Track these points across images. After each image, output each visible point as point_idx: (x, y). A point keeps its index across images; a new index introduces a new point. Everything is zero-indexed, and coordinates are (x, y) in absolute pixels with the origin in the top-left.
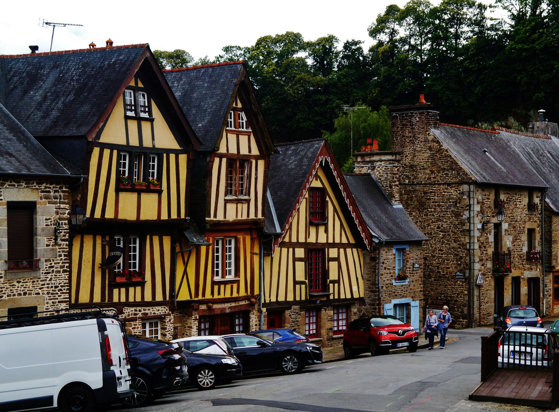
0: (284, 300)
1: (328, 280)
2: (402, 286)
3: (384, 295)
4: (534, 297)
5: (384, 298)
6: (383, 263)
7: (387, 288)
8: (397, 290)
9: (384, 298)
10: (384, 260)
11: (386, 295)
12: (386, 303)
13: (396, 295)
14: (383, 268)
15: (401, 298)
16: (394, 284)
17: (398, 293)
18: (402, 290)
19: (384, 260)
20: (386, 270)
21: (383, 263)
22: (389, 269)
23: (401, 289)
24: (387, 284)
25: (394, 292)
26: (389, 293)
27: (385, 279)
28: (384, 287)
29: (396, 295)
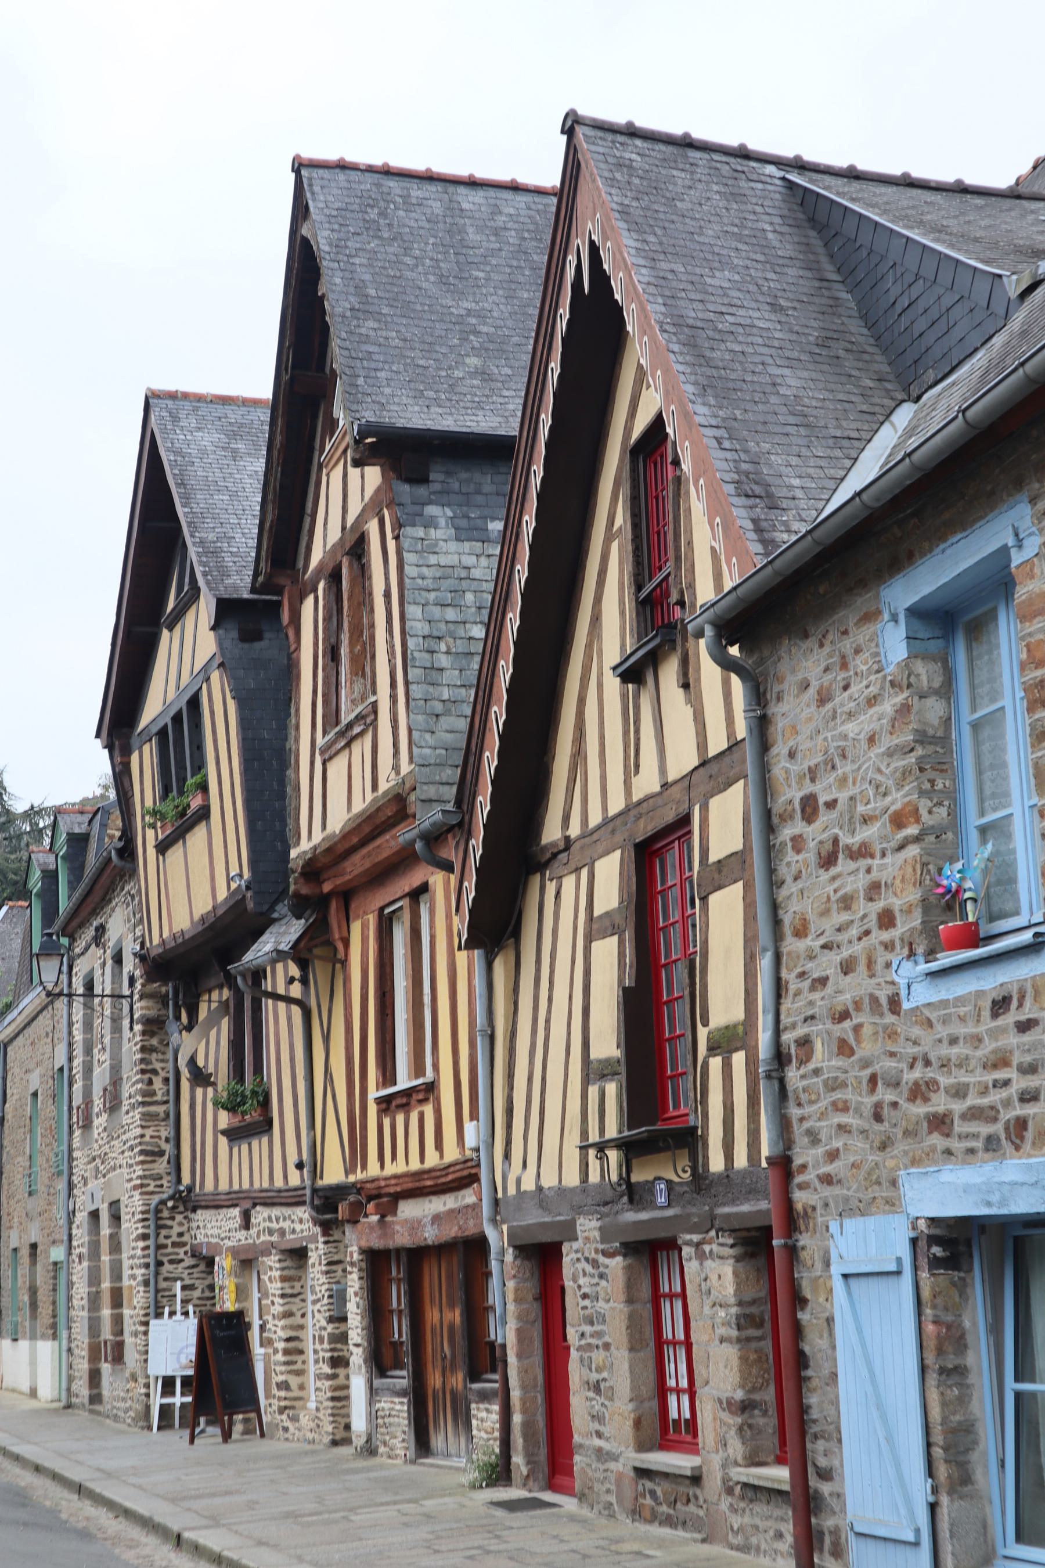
0: (555, 1182)
1: (702, 1033)
2: (1001, 1005)
3: (825, 1127)
4: (659, 944)
5: (833, 1155)
6: (809, 808)
7: (844, 1048)
8: (945, 1065)
9: (833, 1155)
10: (813, 774)
11: (843, 1129)
12: (848, 1210)
13: (940, 1123)
14: (810, 855)
15: (991, 1144)
16: (923, 995)
17: (959, 1092)
18: (1001, 1061)
19: (813, 774)
20: (843, 865)
21: (809, 808)
22: (863, 852)
23: (989, 1046)
24: (844, 1016)
25: (919, 1092)
26: (869, 1101)
27: (828, 964)
28: (818, 1045)
29: (940, 1123)
